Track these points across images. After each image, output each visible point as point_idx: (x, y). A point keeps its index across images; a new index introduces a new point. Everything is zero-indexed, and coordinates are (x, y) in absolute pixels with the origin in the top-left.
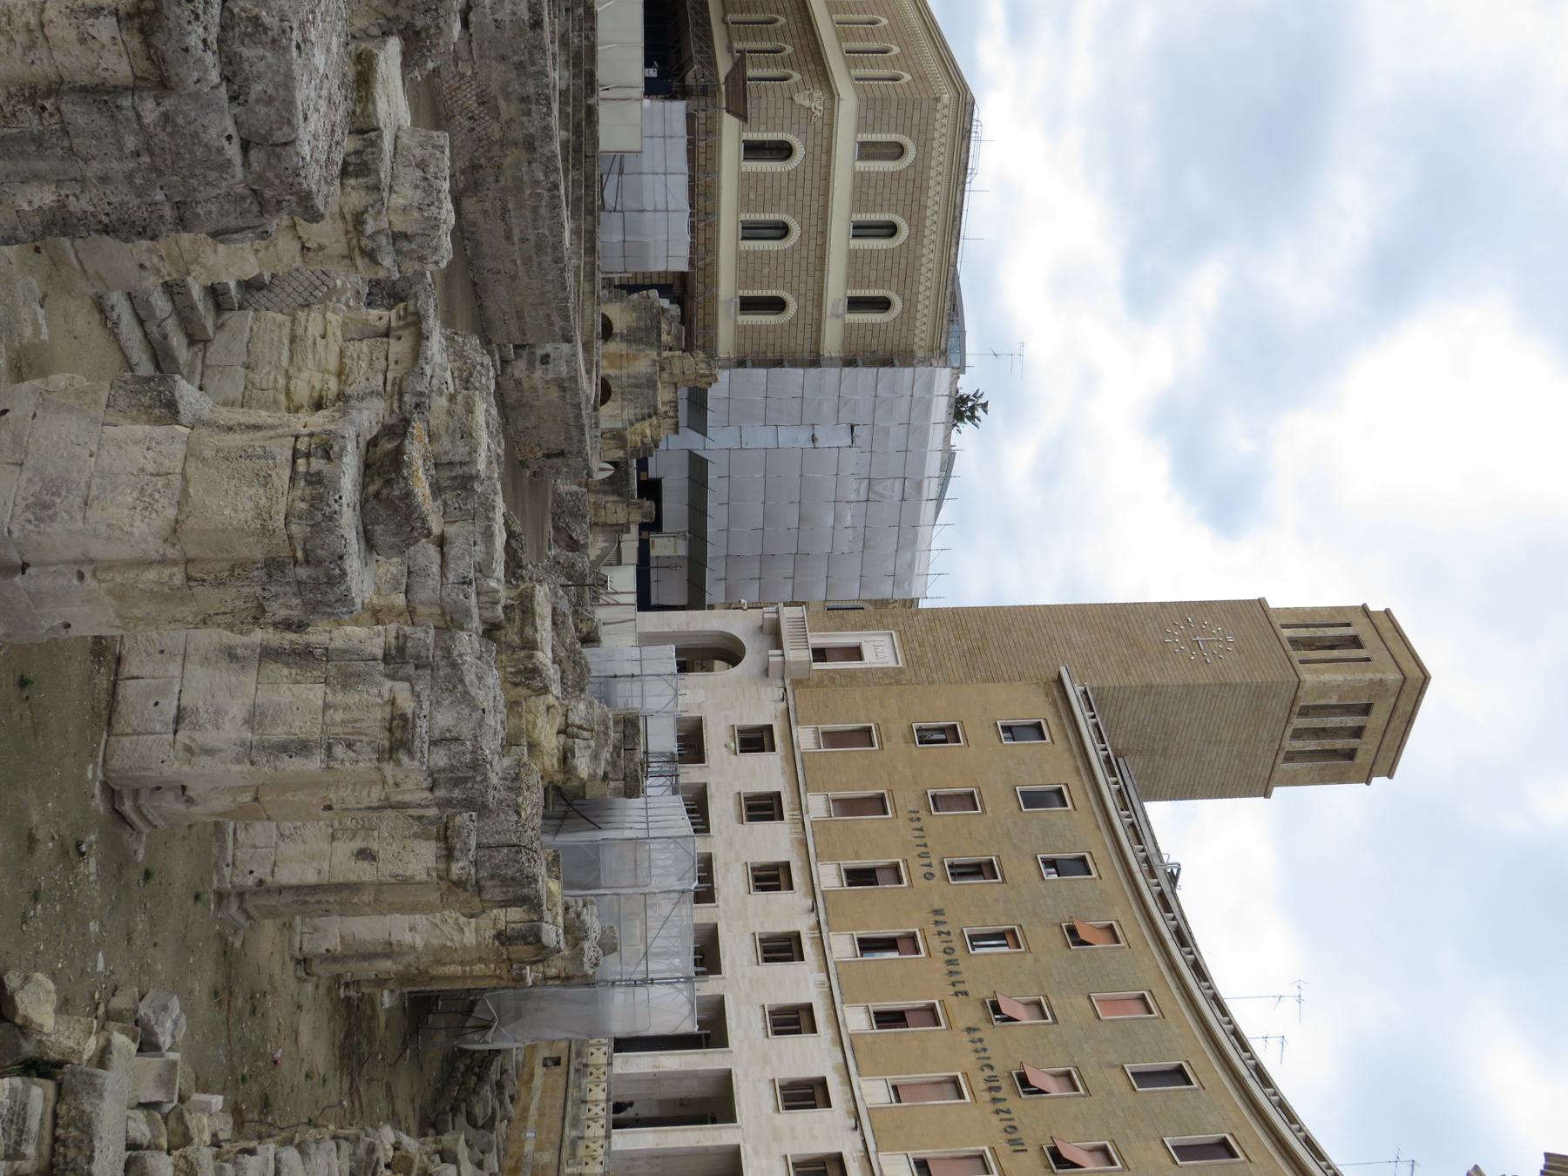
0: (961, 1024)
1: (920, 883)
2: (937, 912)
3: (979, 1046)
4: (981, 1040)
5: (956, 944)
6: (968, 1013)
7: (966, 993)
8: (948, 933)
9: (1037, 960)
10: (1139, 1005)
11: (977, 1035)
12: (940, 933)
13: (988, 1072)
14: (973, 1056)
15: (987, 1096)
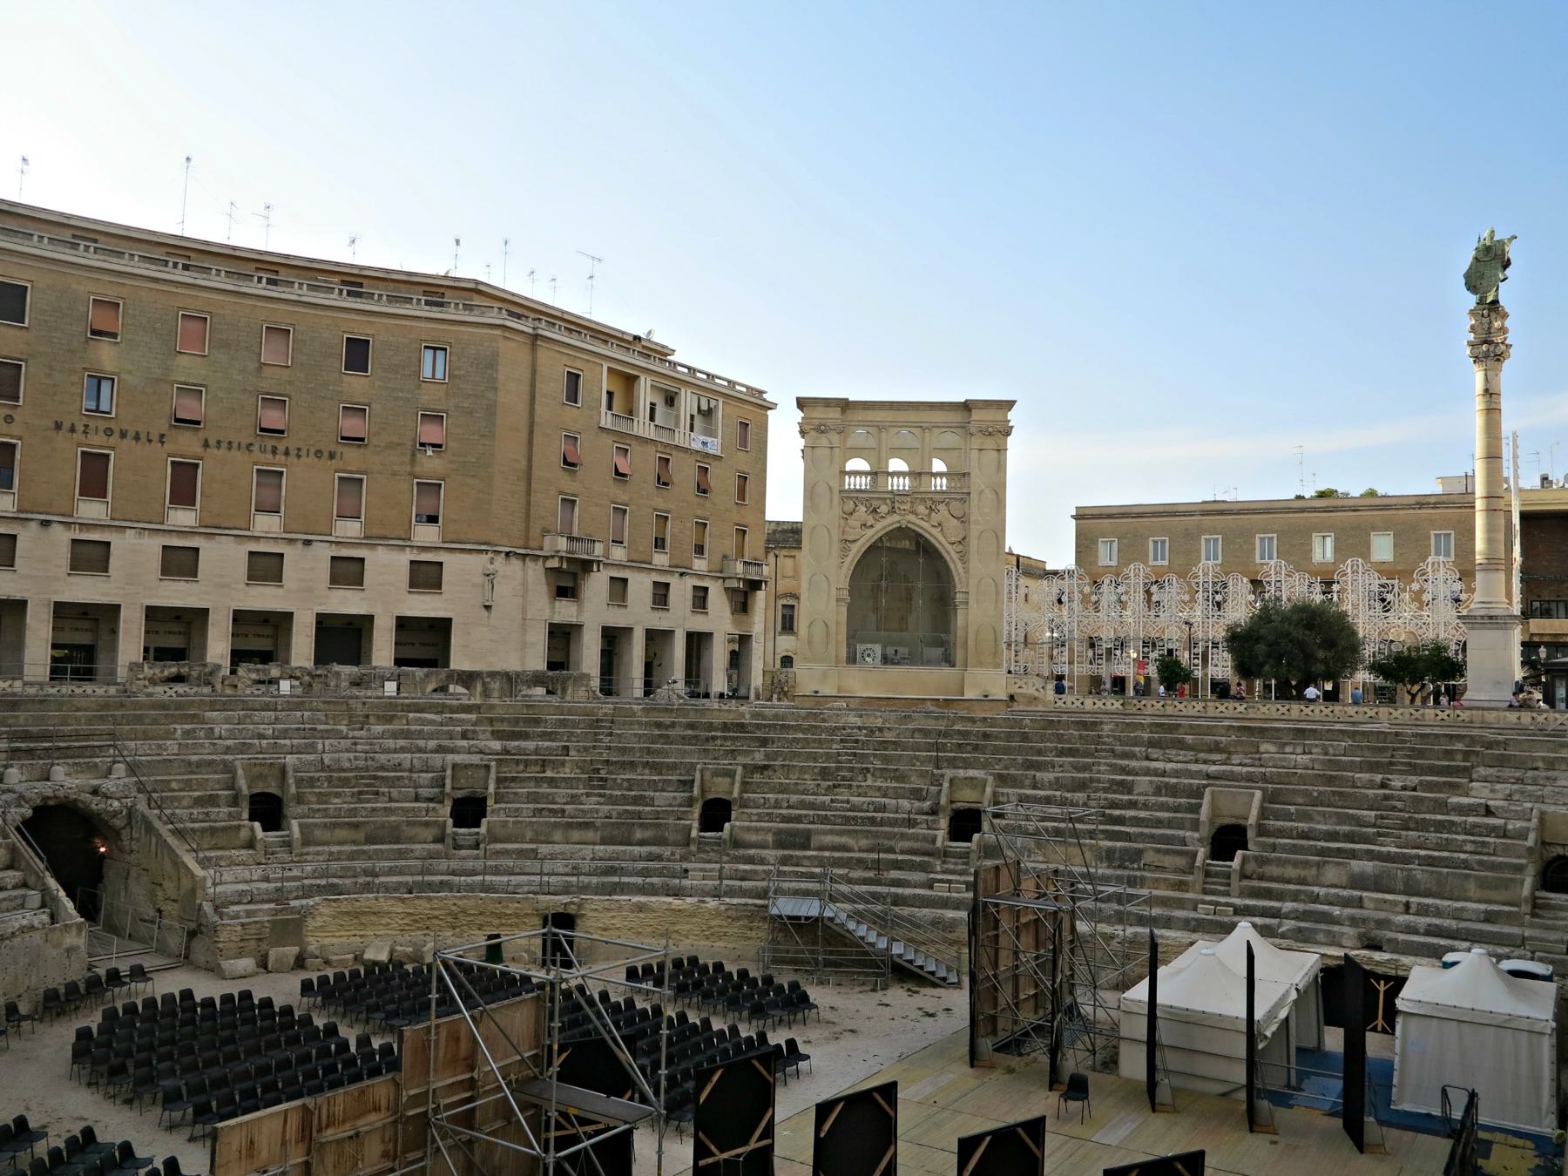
0: (199, 450)
1: (15, 429)
2: (58, 426)
3: (224, 445)
4: (219, 442)
5: (102, 425)
6: (186, 444)
7: (162, 436)
8: (86, 426)
9: (129, 372)
10: (193, 325)
11: (212, 442)
12: (85, 432)
13: (255, 448)
14: (233, 452)
15: (280, 458)
